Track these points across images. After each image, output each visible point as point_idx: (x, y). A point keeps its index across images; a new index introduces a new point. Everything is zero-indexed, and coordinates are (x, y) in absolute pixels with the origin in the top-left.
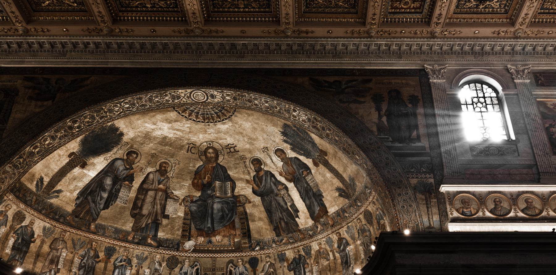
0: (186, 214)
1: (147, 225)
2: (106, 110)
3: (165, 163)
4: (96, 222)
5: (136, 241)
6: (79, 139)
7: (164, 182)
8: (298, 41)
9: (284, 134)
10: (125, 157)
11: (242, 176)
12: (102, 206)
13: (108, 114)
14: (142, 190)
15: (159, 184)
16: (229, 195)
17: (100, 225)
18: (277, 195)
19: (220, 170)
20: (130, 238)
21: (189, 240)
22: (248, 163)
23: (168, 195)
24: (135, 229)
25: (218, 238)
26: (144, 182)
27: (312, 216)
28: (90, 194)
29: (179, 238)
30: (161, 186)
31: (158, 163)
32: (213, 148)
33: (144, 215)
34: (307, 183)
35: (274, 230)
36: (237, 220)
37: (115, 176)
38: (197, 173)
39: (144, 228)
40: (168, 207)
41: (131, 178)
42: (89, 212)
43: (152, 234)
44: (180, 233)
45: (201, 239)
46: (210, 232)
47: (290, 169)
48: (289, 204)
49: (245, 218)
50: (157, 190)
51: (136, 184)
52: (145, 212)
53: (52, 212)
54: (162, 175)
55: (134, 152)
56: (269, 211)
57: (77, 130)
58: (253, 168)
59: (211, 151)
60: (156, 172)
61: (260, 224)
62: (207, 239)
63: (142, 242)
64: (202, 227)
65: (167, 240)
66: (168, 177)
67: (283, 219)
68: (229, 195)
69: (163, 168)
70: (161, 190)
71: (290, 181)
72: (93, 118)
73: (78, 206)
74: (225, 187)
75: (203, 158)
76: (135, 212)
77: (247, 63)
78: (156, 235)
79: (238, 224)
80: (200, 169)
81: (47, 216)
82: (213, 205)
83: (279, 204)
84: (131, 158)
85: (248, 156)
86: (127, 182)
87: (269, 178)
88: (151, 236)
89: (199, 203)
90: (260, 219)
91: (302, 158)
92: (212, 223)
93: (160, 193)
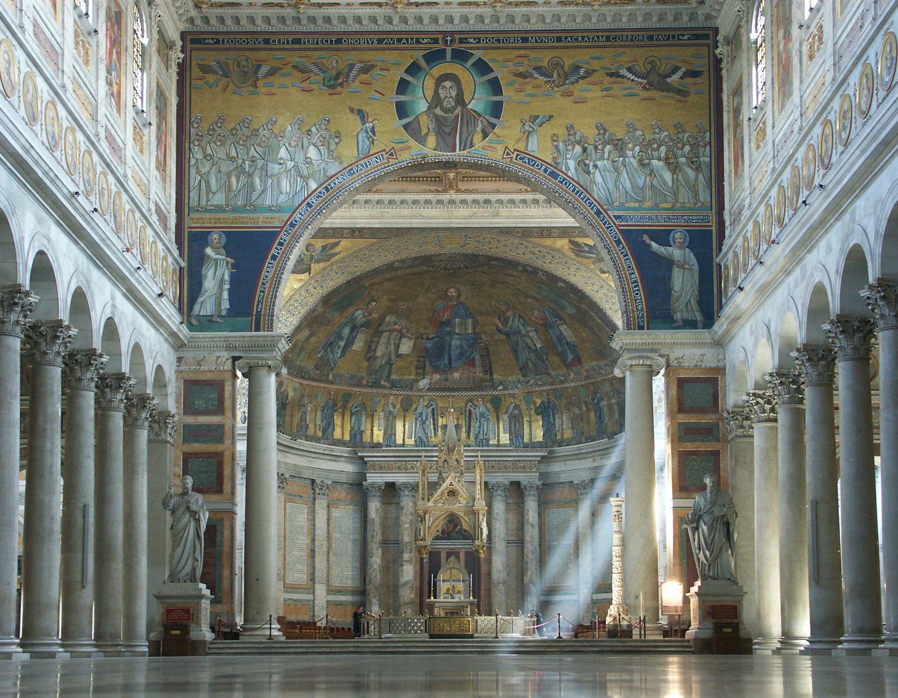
1: (380, 367)
10: (365, 307)
12: (339, 355)
15: (395, 324)
18: (524, 336)
25: (456, 375)
30: (396, 327)
34: (560, 331)
35: (521, 370)
36: (477, 357)
45: (437, 377)
48: (538, 346)
50: (391, 331)
56: (515, 351)
59: (452, 290)
63: (376, 385)
64: (438, 363)
65: (400, 380)
67: (531, 360)
68: (470, 331)
70: (396, 330)
74: (466, 324)
79: (478, 363)
80: (439, 307)
82: (450, 342)
83: (527, 344)
84: (370, 306)
89: (435, 340)
93: (395, 333)
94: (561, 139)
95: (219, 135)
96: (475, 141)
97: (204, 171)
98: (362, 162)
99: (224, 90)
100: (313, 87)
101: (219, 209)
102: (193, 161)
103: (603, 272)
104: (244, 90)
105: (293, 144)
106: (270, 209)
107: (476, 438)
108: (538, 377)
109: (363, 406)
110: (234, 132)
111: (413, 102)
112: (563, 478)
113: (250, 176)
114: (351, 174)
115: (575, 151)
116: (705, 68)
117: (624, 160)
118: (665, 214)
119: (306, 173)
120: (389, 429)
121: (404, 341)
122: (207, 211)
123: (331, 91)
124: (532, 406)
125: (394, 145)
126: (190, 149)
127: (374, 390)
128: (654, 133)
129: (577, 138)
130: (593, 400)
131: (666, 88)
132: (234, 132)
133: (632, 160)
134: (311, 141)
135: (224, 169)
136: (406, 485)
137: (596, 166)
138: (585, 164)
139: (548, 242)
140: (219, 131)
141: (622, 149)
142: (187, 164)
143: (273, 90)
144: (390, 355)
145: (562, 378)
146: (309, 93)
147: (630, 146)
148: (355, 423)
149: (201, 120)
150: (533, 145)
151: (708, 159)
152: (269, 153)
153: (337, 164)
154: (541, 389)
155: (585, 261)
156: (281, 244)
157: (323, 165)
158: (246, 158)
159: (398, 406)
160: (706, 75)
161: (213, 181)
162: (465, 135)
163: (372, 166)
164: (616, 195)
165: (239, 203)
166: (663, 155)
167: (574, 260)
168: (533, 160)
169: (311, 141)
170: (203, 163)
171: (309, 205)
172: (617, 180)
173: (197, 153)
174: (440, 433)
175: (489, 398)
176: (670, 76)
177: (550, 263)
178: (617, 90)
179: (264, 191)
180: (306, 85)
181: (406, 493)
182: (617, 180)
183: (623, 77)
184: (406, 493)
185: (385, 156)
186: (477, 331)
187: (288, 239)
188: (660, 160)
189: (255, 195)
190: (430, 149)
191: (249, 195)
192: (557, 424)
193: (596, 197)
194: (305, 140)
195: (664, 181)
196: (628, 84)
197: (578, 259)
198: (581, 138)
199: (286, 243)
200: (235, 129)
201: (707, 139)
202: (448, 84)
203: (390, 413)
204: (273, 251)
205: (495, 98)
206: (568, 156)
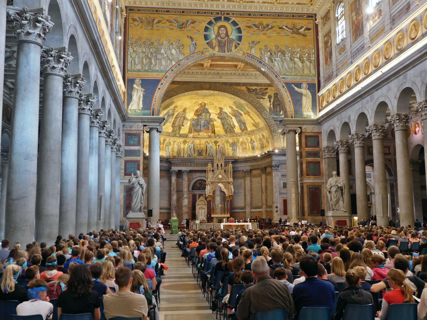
0: (190, 124)
1: (177, 129)
5: (173, 135)
8: (242, 72)
9: (234, 103)
11: (214, 112)
14: (176, 117)
16: (208, 118)
18: (227, 120)
19: (206, 110)
20: (171, 135)
22: (217, 108)
23: (185, 118)
24: (173, 131)
25: (202, 133)
27: (241, 129)
29: (187, 133)
30: (183, 116)
32: (204, 103)
35: (225, 131)
38: (197, 111)
41: (173, 115)
44: (188, 131)
47: (234, 113)
48: (232, 123)
49: (213, 126)
51: (175, 116)
52: (176, 125)
54: (184, 112)
56: (223, 125)
58: (219, 110)
59: (203, 103)
61: (219, 128)
62: (198, 133)
63: (175, 136)
64: (196, 129)
65: (183, 134)
71: (233, 116)
75: (200, 106)
77: (224, 80)
78: (179, 133)
79: (210, 128)
83: (228, 123)
85: (217, 106)
87: (225, 114)
90: (219, 127)
91: (240, 111)
92: (200, 127)
94: (263, 50)
95: (139, 44)
96: (232, 49)
97: (133, 56)
98: (192, 55)
99: (141, 28)
100: (174, 28)
101: (139, 71)
102: (129, 53)
103: (258, 98)
104: (149, 28)
105: (166, 48)
106: (157, 71)
107: (209, 155)
108: (231, 134)
109: (170, 144)
110: (145, 43)
111: (210, 35)
112: (240, 169)
113: (150, 59)
114: (188, 60)
115: (268, 54)
116: (312, 27)
117: (285, 58)
118: (299, 77)
119: (171, 58)
120: (179, 151)
122: (134, 71)
123: (180, 30)
124: (229, 144)
125: (203, 50)
126: (128, 49)
127: (174, 137)
128: (295, 49)
129: (269, 50)
130: (251, 142)
131: (299, 34)
132: (145, 43)
133: (288, 58)
134: (173, 47)
135: (141, 56)
136: (186, 171)
137: (275, 60)
138: (271, 59)
139: (239, 88)
140: (139, 42)
141: (284, 54)
142: (127, 54)
143: (159, 28)
145: (240, 135)
146: (172, 30)
147: (287, 53)
149: (132, 38)
150: (253, 52)
151: (314, 59)
152: (158, 51)
153: (183, 56)
154: (232, 138)
155: (251, 94)
156: (162, 84)
157: (177, 56)
158: (149, 52)
159: (182, 143)
160: (312, 30)
161: (137, 60)
162: (229, 47)
163: (195, 57)
164: (282, 70)
165: (146, 69)
166: (298, 57)
167: (247, 94)
168: (253, 57)
169: (173, 47)
170: (133, 54)
171: (172, 70)
172: (283, 65)
173: (130, 50)
174: (196, 153)
175: (213, 141)
176: (300, 29)
177: (240, 95)
178: (282, 33)
179: (156, 65)
180: (171, 27)
181: (185, 173)
182: (283, 65)
183: (284, 29)
184: (185, 173)
185: (200, 53)
186: (211, 117)
187: (164, 82)
188: (297, 58)
189: (152, 66)
190: (216, 51)
191: (150, 66)
192: (237, 150)
193: (275, 71)
194: (171, 47)
195: (299, 66)
196: (286, 31)
197: (249, 93)
198: (270, 49)
199: (164, 84)
200: (145, 42)
201: (314, 52)
202: (222, 29)
203: (179, 145)
204: (159, 87)
205: (239, 35)
206: (265, 56)
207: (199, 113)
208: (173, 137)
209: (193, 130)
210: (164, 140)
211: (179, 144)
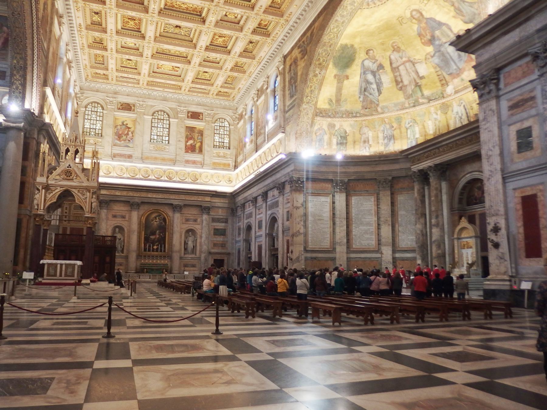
0: (435, 68)
1: (413, 91)
2: (327, 41)
3: (394, 43)
4: (380, 106)
5: (412, 105)
6: (331, 66)
7: (404, 55)
10: (367, 57)
12: (377, 94)
13: (331, 42)
14: (395, 70)
15: (402, 58)
17: (383, 106)
20: (407, 105)
21: (448, 86)
24: (408, 97)
26: (391, 64)
28: (365, 90)
29: (440, 88)
31: (390, 46)
33: (407, 86)
37: (371, 71)
38: (420, 35)
39: (412, 94)
40: (419, 71)
41: (381, 67)
42: (371, 102)
43: (419, 94)
46: (458, 72)
50: (404, 63)
52: (406, 82)
53: (349, 114)
55: (369, 50)
57: (324, 62)
60: (393, 52)
64: (451, 71)
65: (432, 94)
66: (404, 51)
69: (396, 47)
72: (325, 50)
73: (363, 101)
76: (399, 86)
78: (423, 95)
81: (348, 117)
82: (447, 51)
84: (370, 55)
86: (381, 71)
88: (420, 97)
89: (437, 54)
109: (415, 121)
121: (418, 66)
144: (415, 80)
148: (411, 134)
159: (439, 112)
203: (436, 119)
207: (429, 37)
208: (414, 109)
209: (447, 77)
210: (399, 120)
211: (435, 116)
